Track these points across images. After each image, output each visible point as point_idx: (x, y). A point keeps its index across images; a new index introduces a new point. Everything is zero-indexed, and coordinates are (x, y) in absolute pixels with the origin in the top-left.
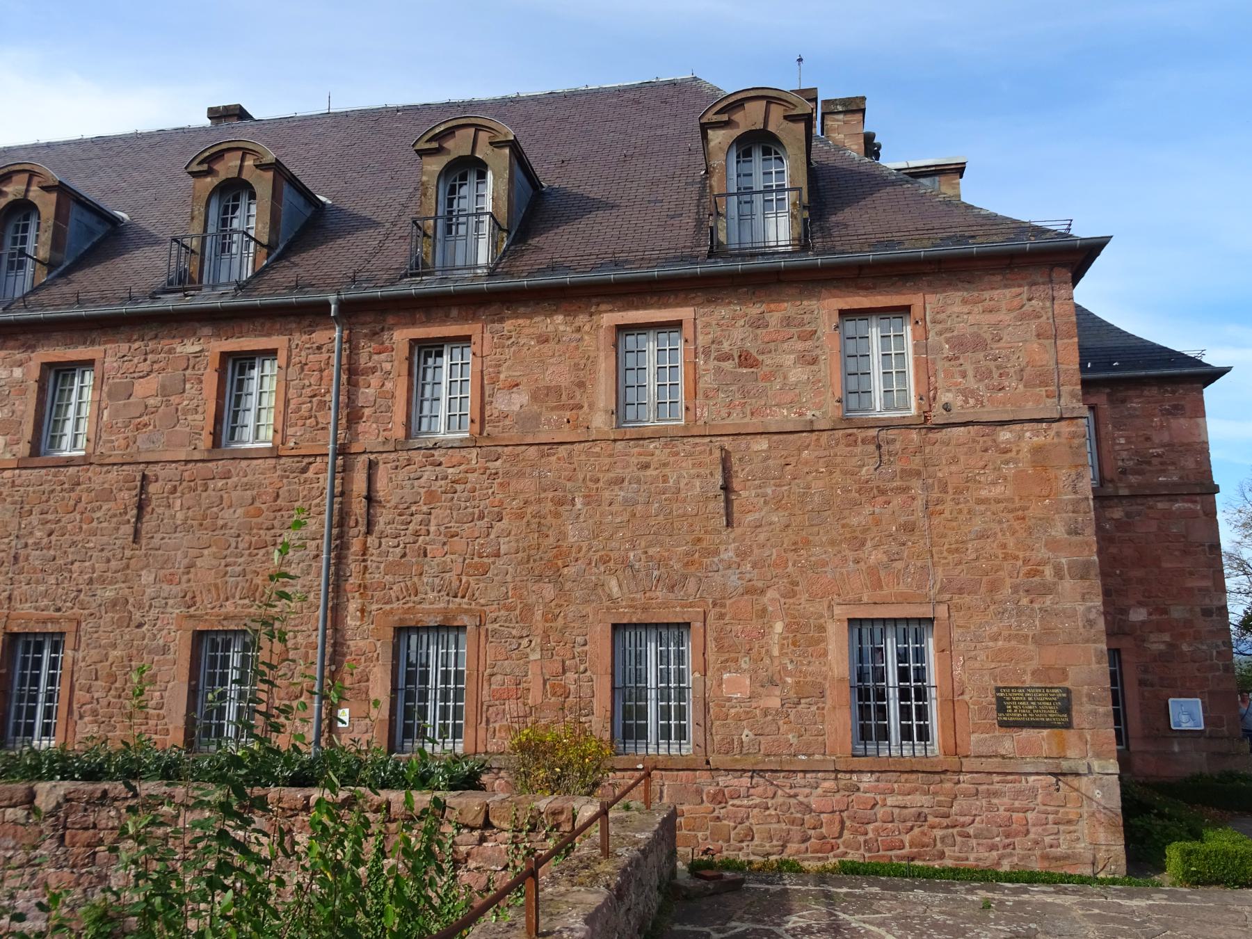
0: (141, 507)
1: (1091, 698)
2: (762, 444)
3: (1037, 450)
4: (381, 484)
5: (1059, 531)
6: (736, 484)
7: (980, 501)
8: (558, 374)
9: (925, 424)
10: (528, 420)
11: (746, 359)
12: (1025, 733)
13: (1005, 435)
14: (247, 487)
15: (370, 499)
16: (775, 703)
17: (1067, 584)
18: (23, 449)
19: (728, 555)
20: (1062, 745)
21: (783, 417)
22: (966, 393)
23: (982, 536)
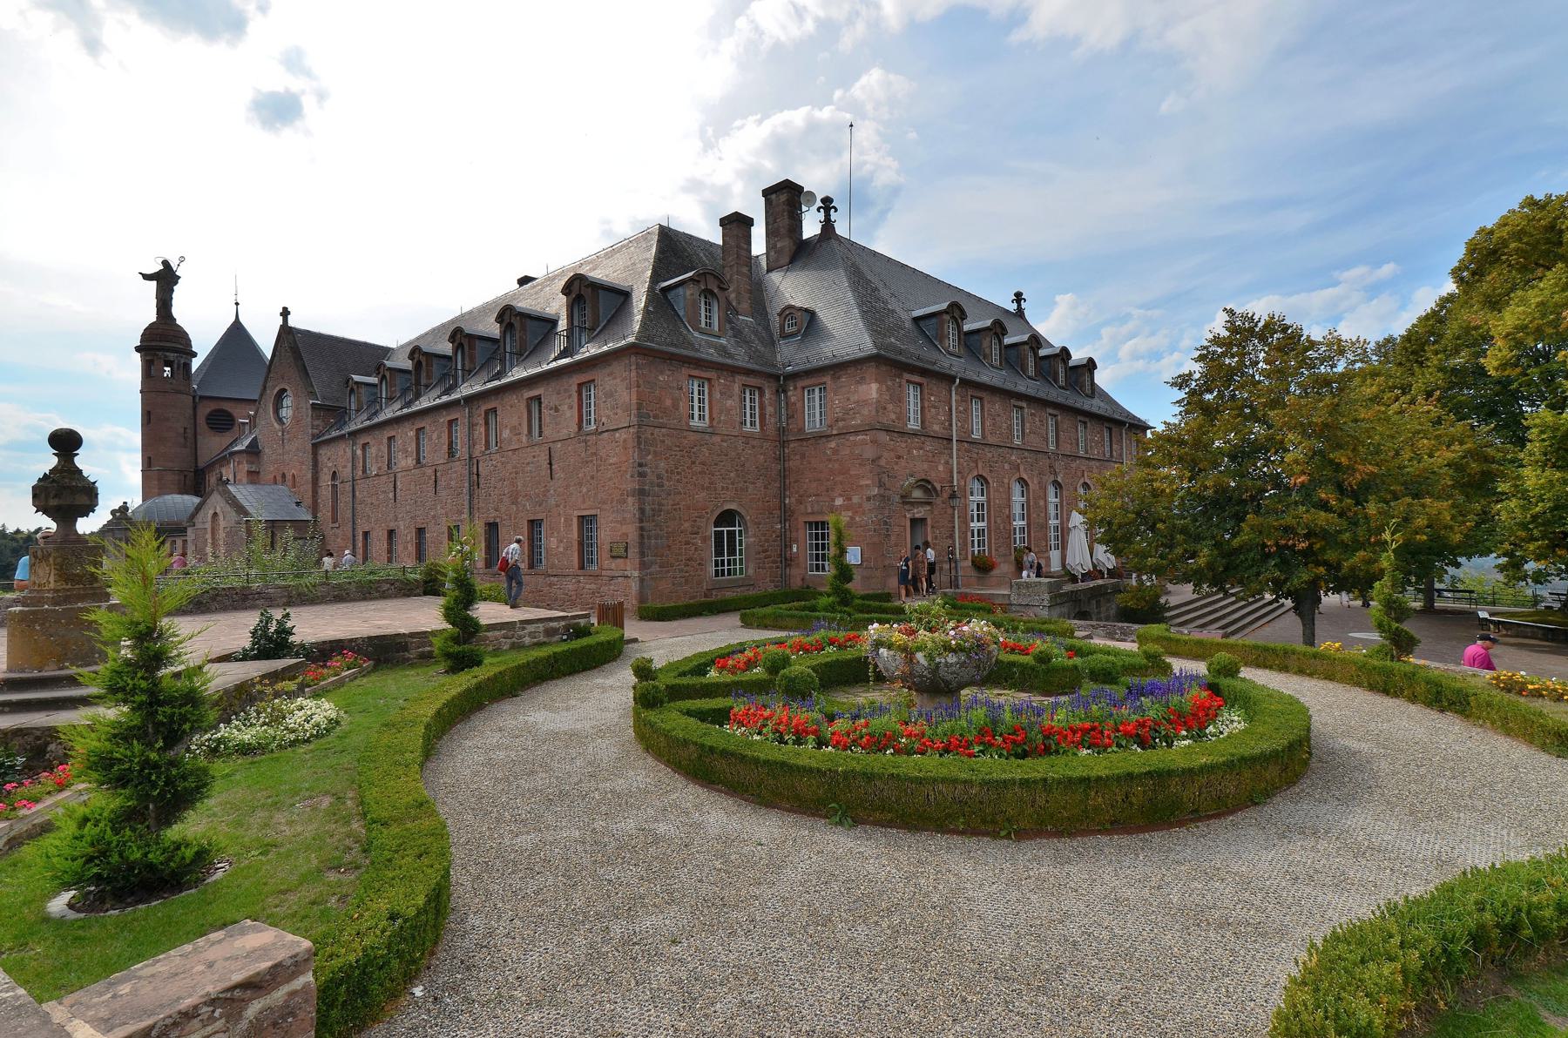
0: (436, 482)
1: (634, 547)
2: (559, 445)
3: (625, 441)
4: (480, 469)
5: (628, 476)
6: (553, 462)
7: (610, 465)
8: (514, 421)
9: (597, 433)
10: (510, 441)
11: (557, 410)
12: (619, 560)
13: (617, 435)
14: (456, 472)
15: (478, 475)
16: (561, 549)
17: (630, 500)
18: (414, 462)
19: (552, 492)
20: (626, 565)
21: (564, 433)
22: (608, 417)
23: (610, 479)
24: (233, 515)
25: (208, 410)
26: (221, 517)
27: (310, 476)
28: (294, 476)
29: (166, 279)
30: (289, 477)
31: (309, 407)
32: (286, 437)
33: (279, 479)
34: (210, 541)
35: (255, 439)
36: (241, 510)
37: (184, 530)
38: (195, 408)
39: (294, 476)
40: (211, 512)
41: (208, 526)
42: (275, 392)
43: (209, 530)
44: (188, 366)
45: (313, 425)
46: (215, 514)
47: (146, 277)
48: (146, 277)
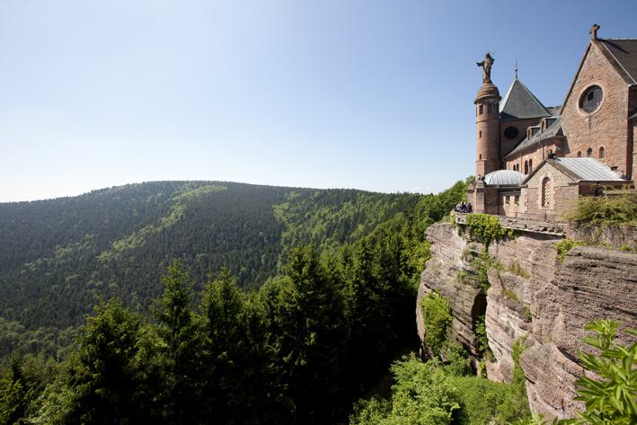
24: (565, 180)
25: (506, 128)
26: (552, 180)
27: (624, 145)
28: (602, 149)
29: (487, 64)
30: (596, 150)
31: (627, 89)
32: (594, 121)
33: (584, 152)
34: (540, 196)
35: (560, 132)
36: (571, 174)
37: (519, 190)
38: (500, 127)
39: (602, 149)
40: (542, 178)
41: (540, 186)
42: (582, 92)
43: (541, 189)
44: (498, 106)
45: (629, 104)
46: (546, 179)
47: (479, 65)
48: (479, 65)
